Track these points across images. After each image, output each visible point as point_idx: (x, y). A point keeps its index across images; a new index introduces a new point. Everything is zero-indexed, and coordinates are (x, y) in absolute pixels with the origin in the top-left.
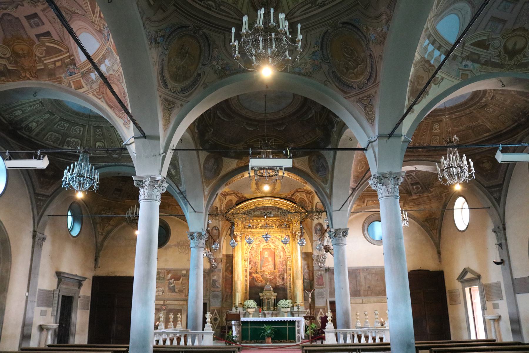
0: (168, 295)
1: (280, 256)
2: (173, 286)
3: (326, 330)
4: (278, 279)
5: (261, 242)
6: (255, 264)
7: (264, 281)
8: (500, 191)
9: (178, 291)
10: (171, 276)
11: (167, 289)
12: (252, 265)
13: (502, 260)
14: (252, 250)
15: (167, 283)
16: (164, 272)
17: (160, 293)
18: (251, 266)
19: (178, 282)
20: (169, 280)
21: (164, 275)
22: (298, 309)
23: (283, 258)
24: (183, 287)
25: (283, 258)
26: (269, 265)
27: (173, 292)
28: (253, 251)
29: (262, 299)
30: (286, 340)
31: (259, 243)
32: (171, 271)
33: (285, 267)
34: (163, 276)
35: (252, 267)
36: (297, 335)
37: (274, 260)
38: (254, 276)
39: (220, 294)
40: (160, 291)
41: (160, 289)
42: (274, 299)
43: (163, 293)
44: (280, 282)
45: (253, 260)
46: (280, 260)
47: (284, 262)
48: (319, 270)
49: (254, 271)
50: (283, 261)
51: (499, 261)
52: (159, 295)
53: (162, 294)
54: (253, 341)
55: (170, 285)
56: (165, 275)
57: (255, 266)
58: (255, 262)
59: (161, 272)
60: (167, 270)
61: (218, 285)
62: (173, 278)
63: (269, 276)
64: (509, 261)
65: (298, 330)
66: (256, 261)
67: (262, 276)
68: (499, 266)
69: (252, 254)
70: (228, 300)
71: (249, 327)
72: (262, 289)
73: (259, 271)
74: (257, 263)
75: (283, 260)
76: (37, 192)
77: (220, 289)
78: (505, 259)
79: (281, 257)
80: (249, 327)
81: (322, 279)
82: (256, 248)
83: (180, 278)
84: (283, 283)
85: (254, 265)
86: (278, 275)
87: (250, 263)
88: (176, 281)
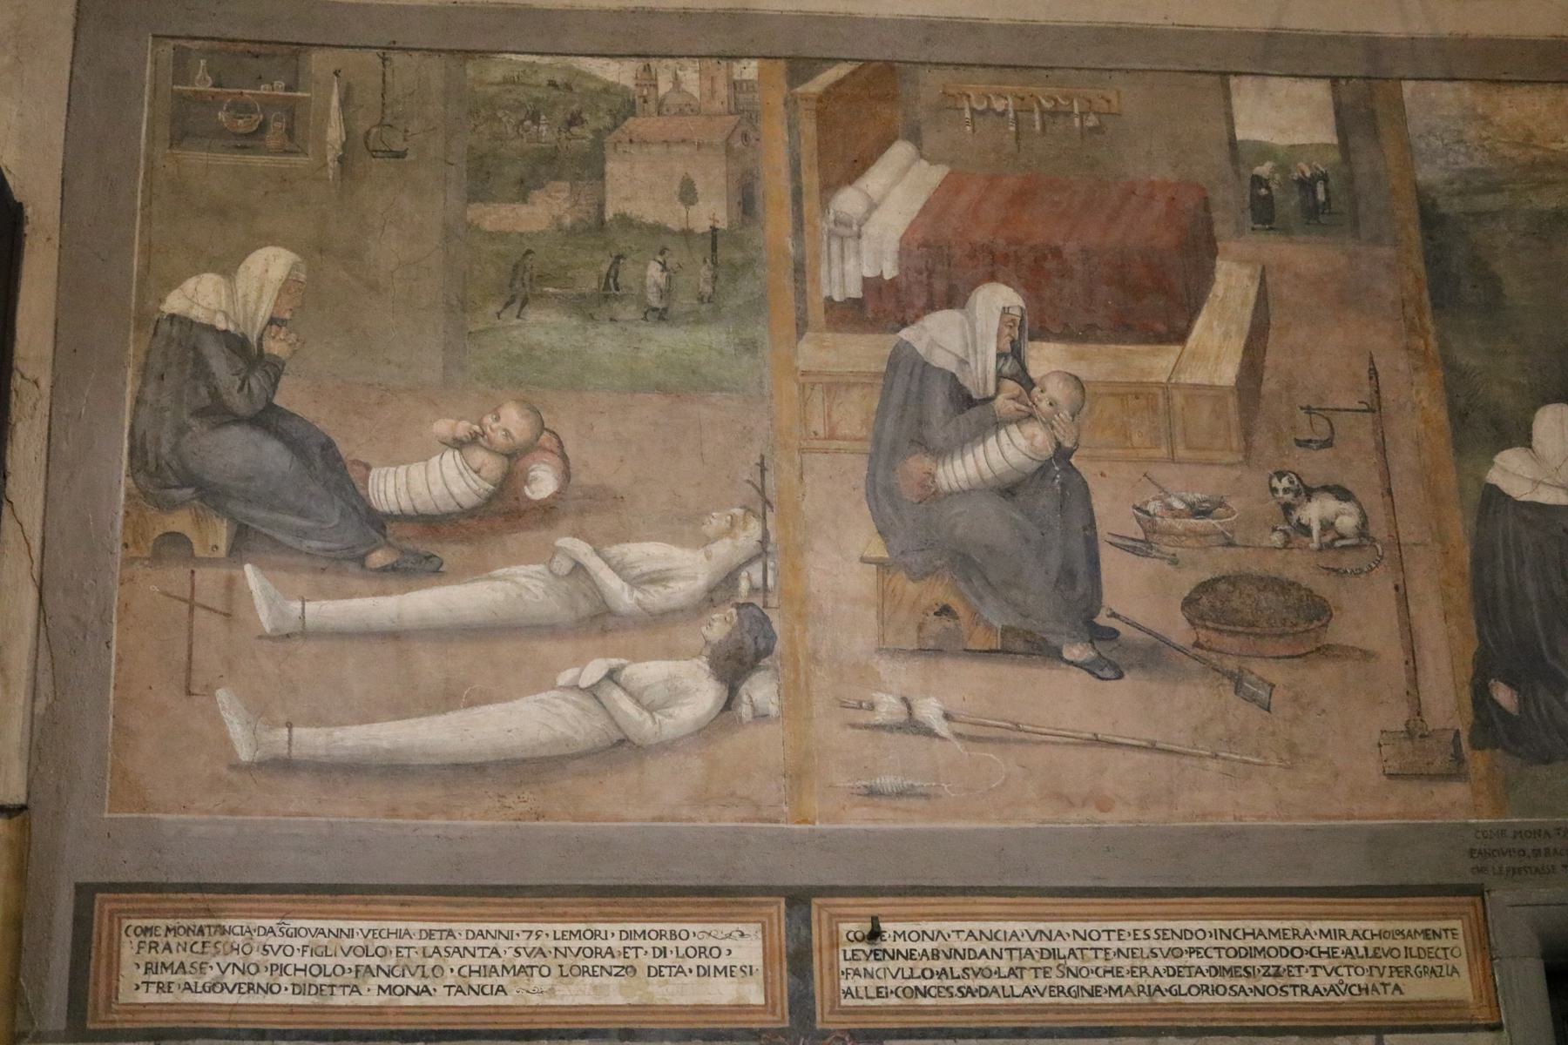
0: (913, 726)
2: (1009, 489)
9: (1179, 630)
10: (935, 209)
15: (835, 386)
16: (745, 115)
17: (649, 672)
19: (1157, 363)
21: (747, 202)
24: (1313, 512)
27: (1040, 650)
32: (932, 83)
34: (711, 212)
40: (657, 620)
41: (646, 553)
53: (729, 705)
55: (941, 453)
56: (775, 186)
59: (625, 106)
60: (800, 67)
62: (993, 265)
83: (1206, 277)
88: (1066, 335)
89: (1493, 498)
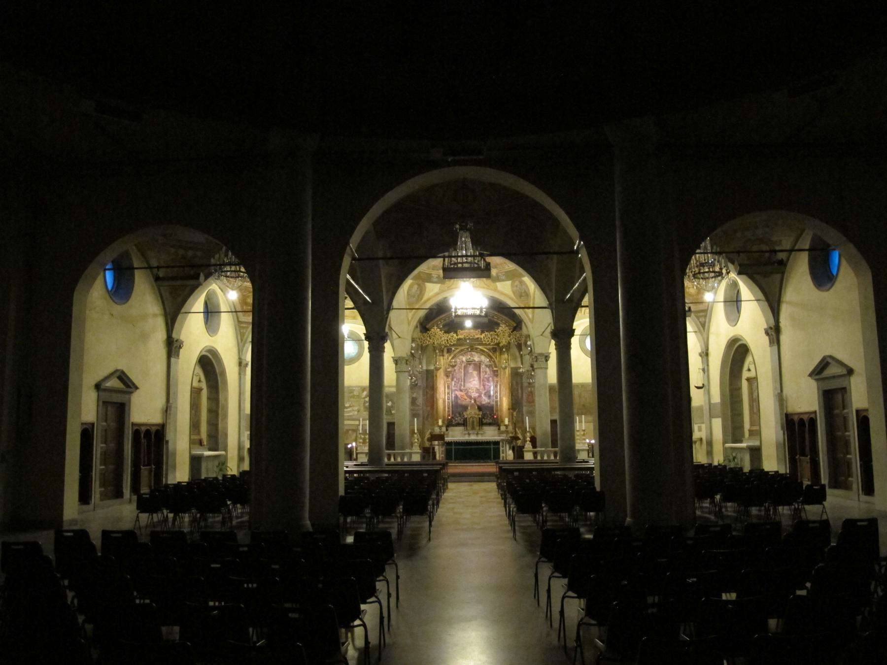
1: (486, 372)
3: (525, 449)
6: (459, 381)
7: (468, 400)
8: (705, 316)
11: (362, 408)
12: (455, 382)
13: (703, 384)
18: (453, 383)
20: (364, 398)
22: (506, 428)
26: (474, 380)
29: (466, 418)
30: (491, 460)
35: (455, 384)
36: (501, 455)
38: (458, 395)
39: (421, 412)
42: (479, 418)
43: (358, 412)
44: (485, 400)
46: (486, 376)
48: (529, 387)
50: (489, 378)
51: (701, 385)
52: (354, 415)
54: (457, 461)
57: (458, 383)
59: (354, 390)
61: (418, 404)
64: (709, 386)
65: (503, 451)
67: (466, 394)
68: (702, 390)
70: (429, 419)
71: (453, 447)
72: (465, 408)
73: (462, 387)
75: (489, 376)
76: (240, 320)
77: (421, 408)
78: (706, 384)
79: (487, 374)
80: (453, 447)
81: (532, 396)
84: (489, 401)
86: (484, 393)
87: (452, 380)
89: (387, 405)
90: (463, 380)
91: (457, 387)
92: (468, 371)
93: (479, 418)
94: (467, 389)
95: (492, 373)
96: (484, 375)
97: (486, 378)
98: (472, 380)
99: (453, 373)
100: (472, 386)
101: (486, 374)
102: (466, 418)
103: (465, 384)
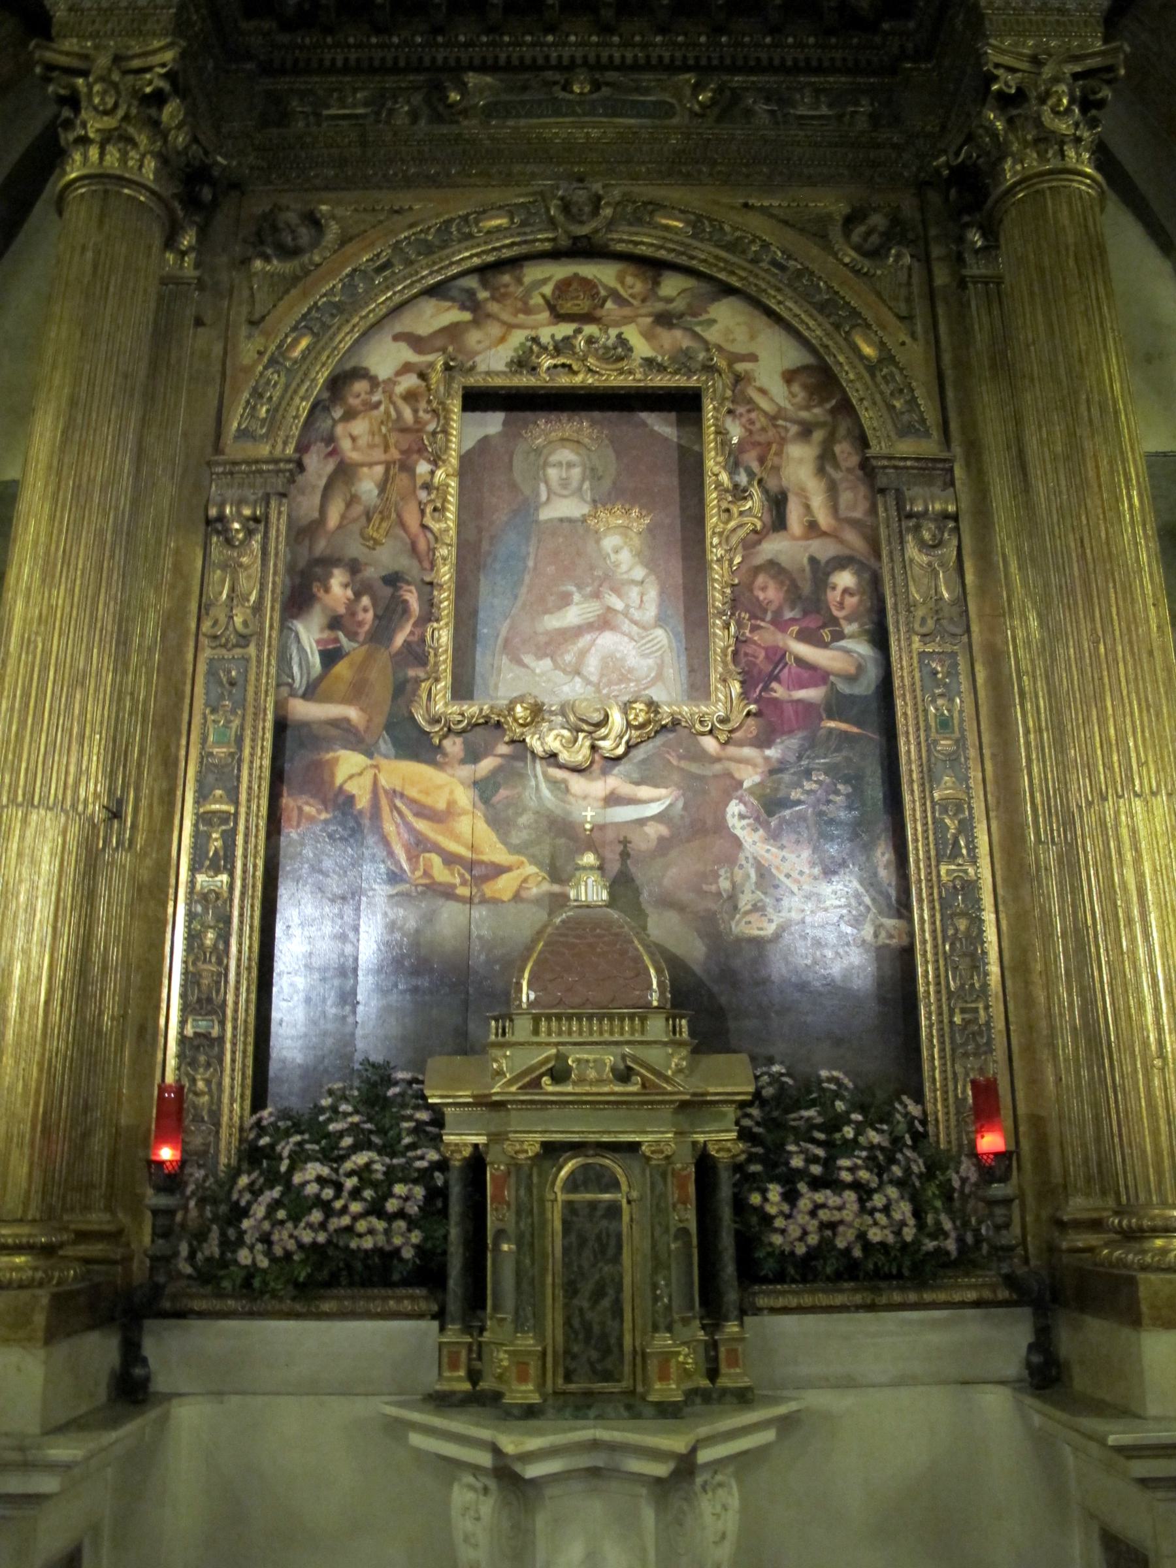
1: (778, 503)
4: (753, 841)
5: (493, 307)
12: (335, 623)
14: (350, 415)
23: (824, 519)
25: (824, 519)
28: (359, 427)
31: (454, 315)
33: (863, 649)
35: (330, 657)
37: (676, 567)
45: (355, 549)
46: (774, 547)
47: (845, 579)
49: (352, 713)
50: (821, 572)
57: (381, 632)
58: (393, 580)
63: (598, 787)
66: (405, 563)
69: (344, 472)
74: (412, 599)
75: (824, 550)
82: (410, 381)
85: (370, 615)
86: (751, 778)
90: (445, 600)
91: (356, 693)
92: (526, 509)
93: (705, 1164)
94: (493, 725)
95: (854, 501)
96: (751, 543)
97: (773, 567)
98: (572, 616)
99: (308, 506)
100: (572, 690)
101: (779, 523)
102: (477, 1162)
103: (482, 660)
